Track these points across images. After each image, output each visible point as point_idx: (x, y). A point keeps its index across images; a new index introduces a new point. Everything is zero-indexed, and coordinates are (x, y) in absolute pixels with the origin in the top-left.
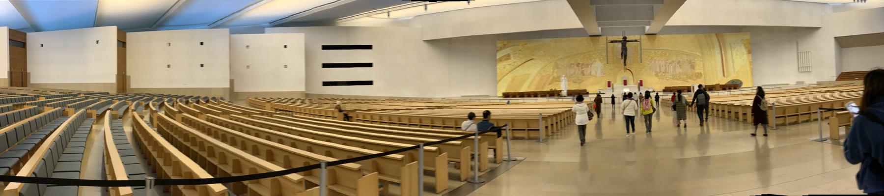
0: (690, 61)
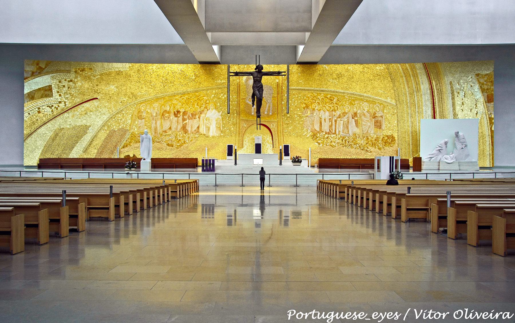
0: (375, 113)
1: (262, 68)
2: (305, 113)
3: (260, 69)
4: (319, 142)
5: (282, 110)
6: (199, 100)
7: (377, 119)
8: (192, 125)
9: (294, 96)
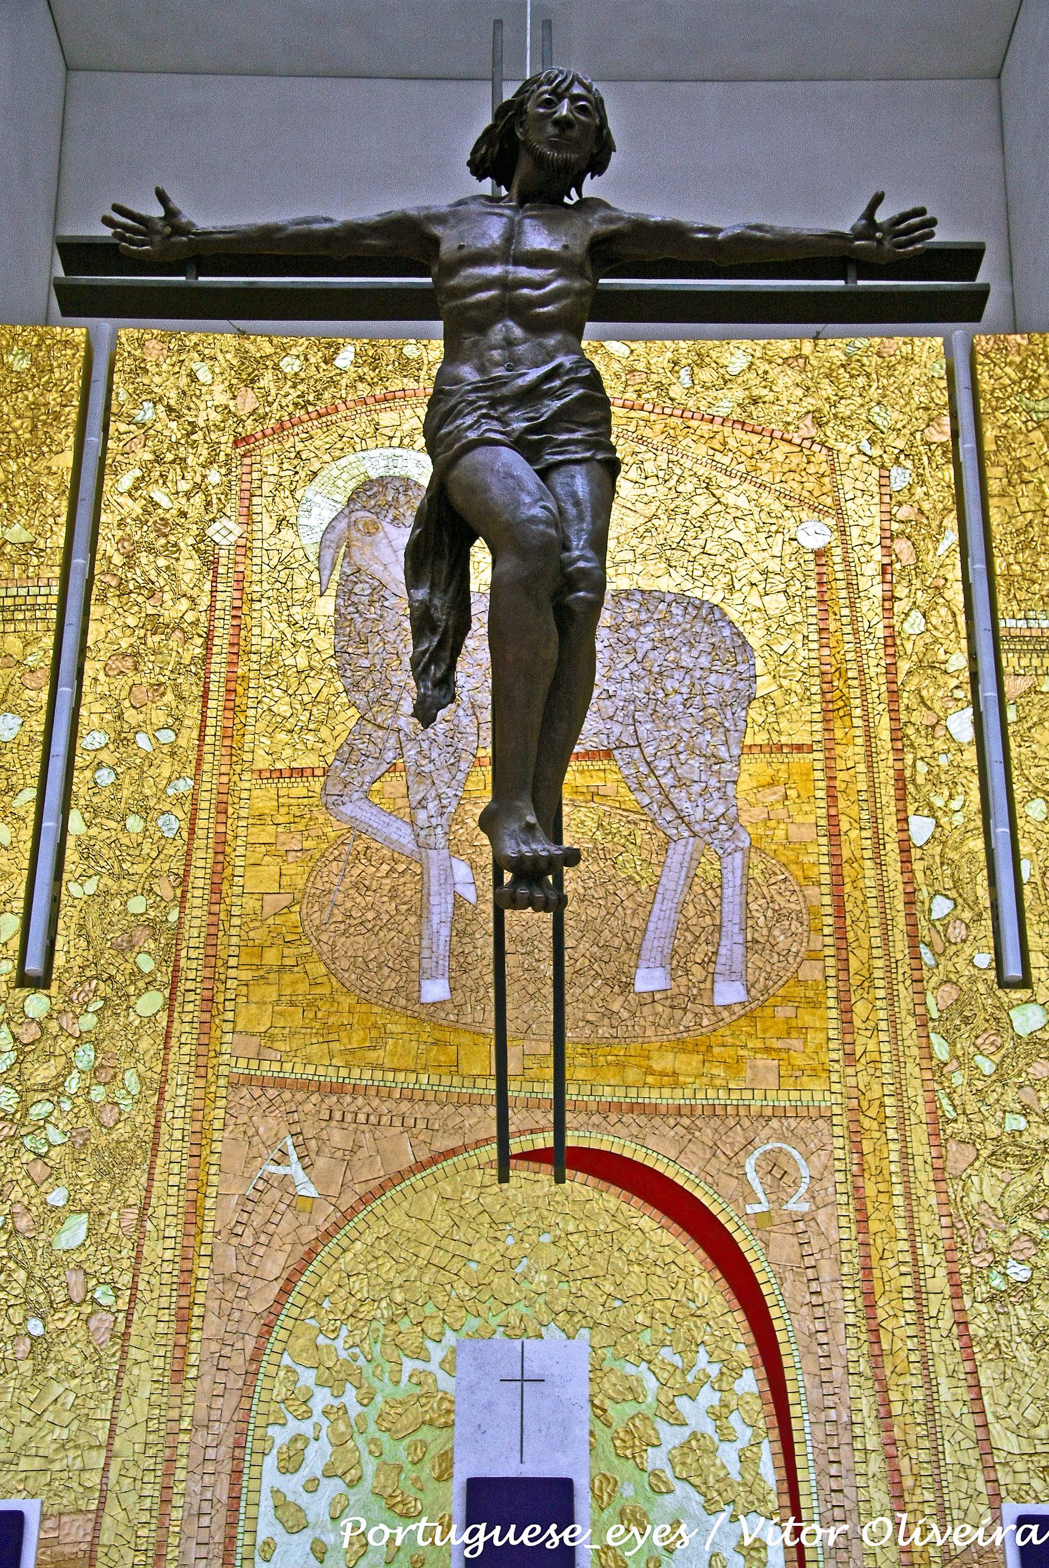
1: (598, 165)
5: (914, 939)
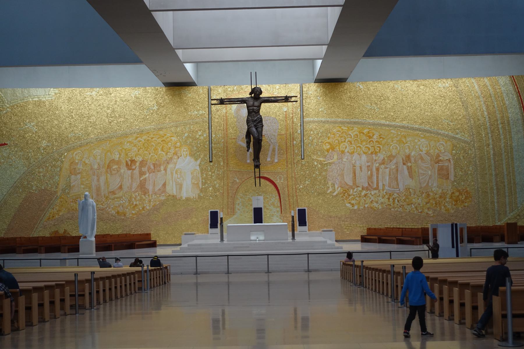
0: (438, 156)
1: (261, 92)
2: (329, 159)
3: (257, 94)
4: (353, 202)
6: (164, 142)
7: (442, 165)
8: (154, 182)
9: (312, 132)
